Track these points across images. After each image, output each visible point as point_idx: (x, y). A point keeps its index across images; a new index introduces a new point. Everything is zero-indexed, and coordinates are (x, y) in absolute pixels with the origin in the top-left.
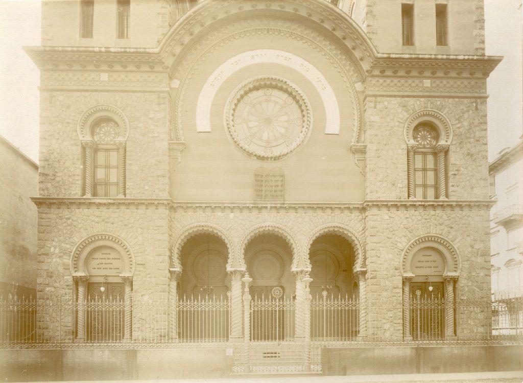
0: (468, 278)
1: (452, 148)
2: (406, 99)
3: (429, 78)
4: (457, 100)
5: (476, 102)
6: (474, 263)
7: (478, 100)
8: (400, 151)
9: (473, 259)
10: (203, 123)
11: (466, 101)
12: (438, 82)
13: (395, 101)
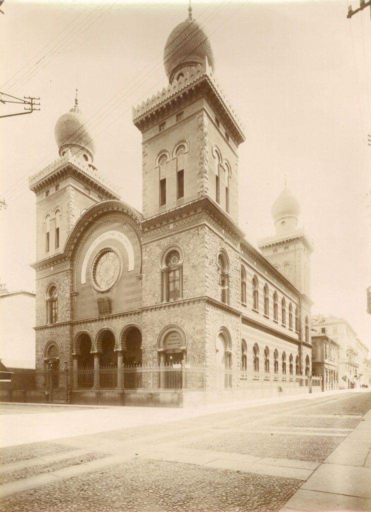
0: (192, 349)
1: (184, 265)
2: (161, 240)
3: (172, 223)
4: (187, 232)
5: (198, 230)
6: (195, 340)
7: (199, 228)
8: (157, 274)
9: (194, 337)
10: (83, 281)
11: (192, 231)
12: (177, 223)
13: (155, 244)
